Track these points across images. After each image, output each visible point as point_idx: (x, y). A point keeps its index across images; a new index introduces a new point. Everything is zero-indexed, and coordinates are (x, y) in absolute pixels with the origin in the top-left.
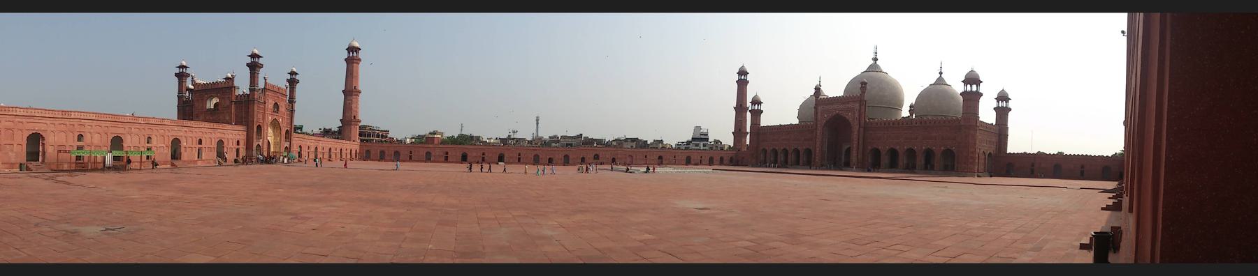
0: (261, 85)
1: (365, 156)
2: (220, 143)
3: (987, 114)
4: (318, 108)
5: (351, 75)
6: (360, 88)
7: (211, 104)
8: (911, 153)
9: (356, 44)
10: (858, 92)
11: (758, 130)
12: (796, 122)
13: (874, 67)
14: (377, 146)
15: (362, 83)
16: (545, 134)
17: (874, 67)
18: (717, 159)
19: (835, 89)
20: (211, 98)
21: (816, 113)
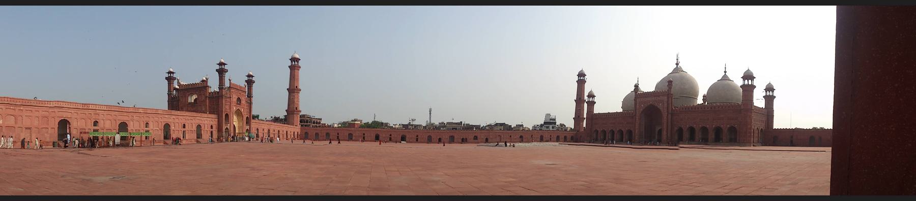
0: (227, 84)
1: (304, 136)
2: (199, 127)
3: (759, 101)
4: (269, 102)
5: (293, 78)
6: (300, 87)
7: (192, 99)
8: (704, 130)
9: (297, 56)
10: (666, 88)
11: (592, 117)
12: (621, 110)
13: (677, 69)
14: (312, 129)
15: (302, 83)
16: (436, 121)
17: (677, 69)
18: (562, 137)
19: (648, 87)
20: (192, 94)
21: (636, 104)
